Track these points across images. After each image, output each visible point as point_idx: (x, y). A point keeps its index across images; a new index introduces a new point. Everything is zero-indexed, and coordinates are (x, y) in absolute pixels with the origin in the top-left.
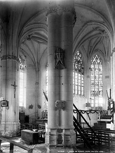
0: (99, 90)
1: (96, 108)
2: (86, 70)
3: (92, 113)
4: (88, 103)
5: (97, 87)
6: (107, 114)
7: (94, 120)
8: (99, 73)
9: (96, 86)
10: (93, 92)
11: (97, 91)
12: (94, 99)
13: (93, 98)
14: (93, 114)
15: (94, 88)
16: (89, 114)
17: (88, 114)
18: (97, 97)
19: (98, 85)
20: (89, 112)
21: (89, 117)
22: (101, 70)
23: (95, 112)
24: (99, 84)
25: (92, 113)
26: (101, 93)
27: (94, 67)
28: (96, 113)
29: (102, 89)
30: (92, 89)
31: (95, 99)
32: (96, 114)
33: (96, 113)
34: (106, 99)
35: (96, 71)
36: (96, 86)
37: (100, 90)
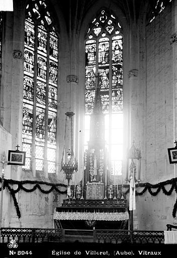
0: (46, 114)
1: (38, 173)
2: (12, 28)
3: (43, 192)
4: (17, 151)
5: (41, 105)
6: (84, 196)
7: (32, 217)
8: (50, 61)
9: (39, 100)
10: (31, 116)
11: (40, 117)
12: (30, 142)
13: (28, 136)
14: (29, 194)
15: (32, 103)
16: (17, 195)
17: (13, 193)
18: (41, 135)
19: (45, 98)
20: (15, 187)
21: (16, 204)
22: (55, 53)
23: (144, 191)
24: (47, 93)
25: (43, 192)
26: (52, 125)
27: (33, 31)
28: (37, 190)
29: (54, 115)
30: (27, 106)
31: (37, 143)
32: (38, 195)
33: (37, 190)
34: (129, 111)
35: (40, 48)
36: (39, 100)
37: (49, 117)
